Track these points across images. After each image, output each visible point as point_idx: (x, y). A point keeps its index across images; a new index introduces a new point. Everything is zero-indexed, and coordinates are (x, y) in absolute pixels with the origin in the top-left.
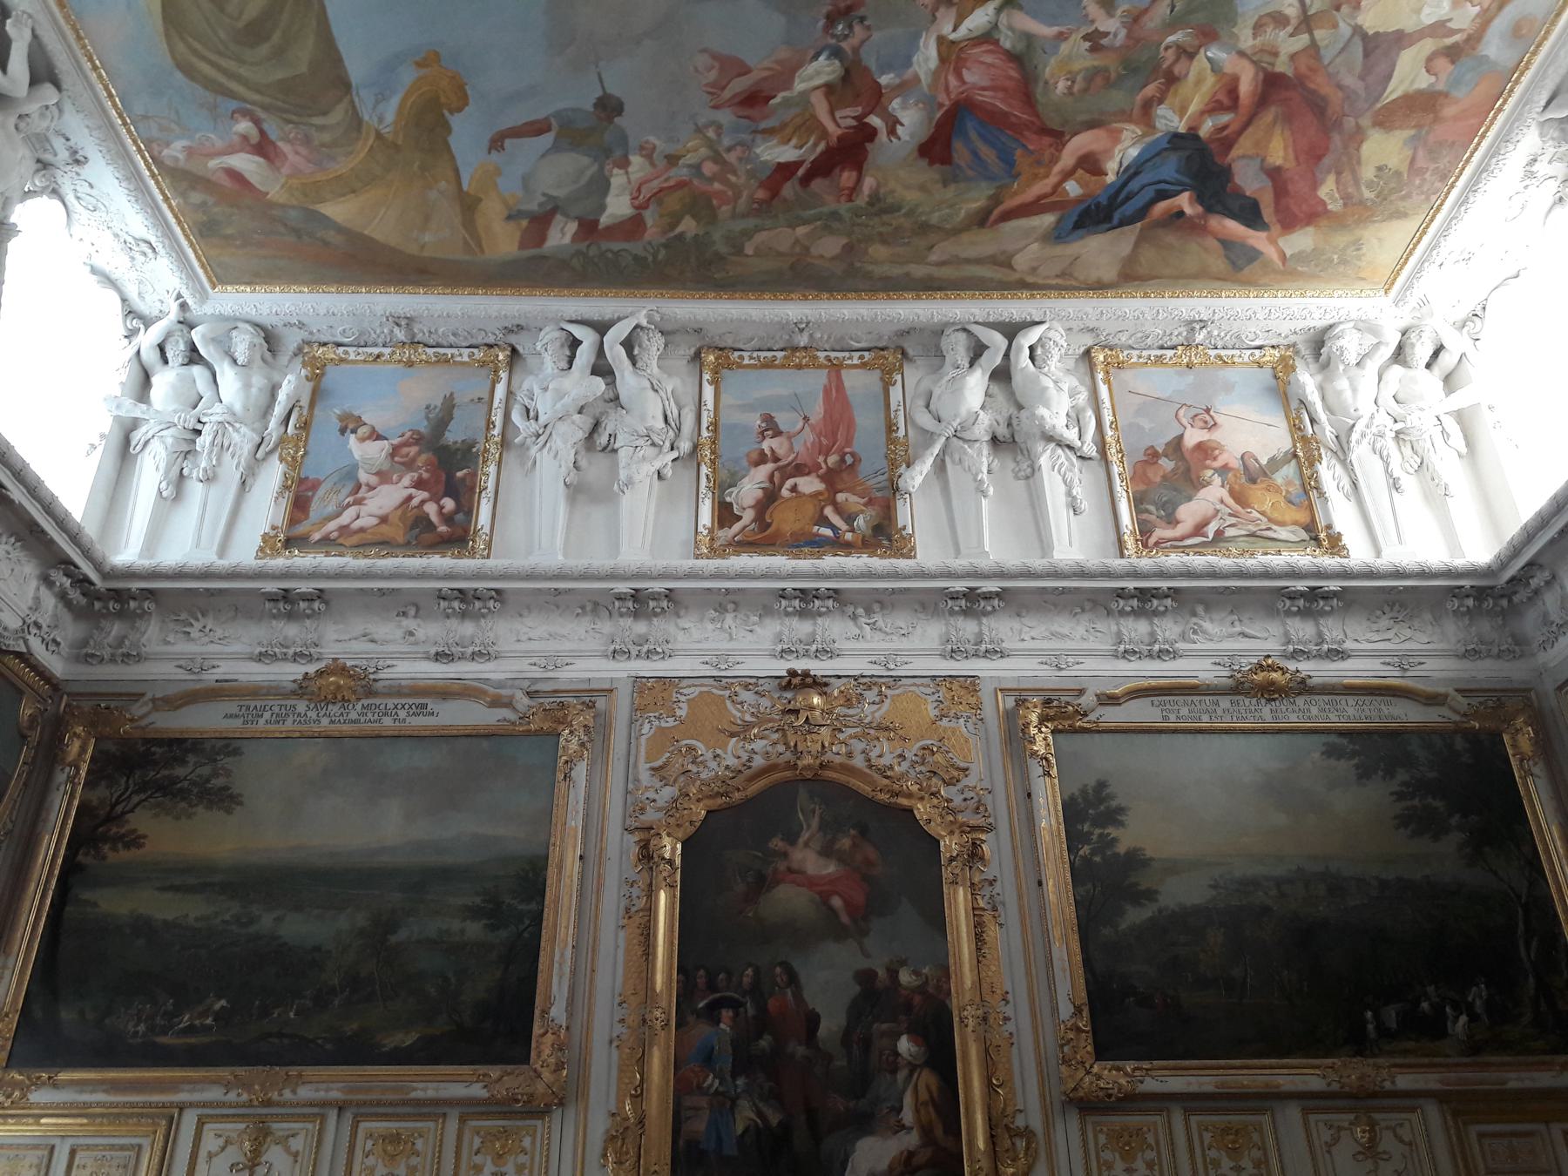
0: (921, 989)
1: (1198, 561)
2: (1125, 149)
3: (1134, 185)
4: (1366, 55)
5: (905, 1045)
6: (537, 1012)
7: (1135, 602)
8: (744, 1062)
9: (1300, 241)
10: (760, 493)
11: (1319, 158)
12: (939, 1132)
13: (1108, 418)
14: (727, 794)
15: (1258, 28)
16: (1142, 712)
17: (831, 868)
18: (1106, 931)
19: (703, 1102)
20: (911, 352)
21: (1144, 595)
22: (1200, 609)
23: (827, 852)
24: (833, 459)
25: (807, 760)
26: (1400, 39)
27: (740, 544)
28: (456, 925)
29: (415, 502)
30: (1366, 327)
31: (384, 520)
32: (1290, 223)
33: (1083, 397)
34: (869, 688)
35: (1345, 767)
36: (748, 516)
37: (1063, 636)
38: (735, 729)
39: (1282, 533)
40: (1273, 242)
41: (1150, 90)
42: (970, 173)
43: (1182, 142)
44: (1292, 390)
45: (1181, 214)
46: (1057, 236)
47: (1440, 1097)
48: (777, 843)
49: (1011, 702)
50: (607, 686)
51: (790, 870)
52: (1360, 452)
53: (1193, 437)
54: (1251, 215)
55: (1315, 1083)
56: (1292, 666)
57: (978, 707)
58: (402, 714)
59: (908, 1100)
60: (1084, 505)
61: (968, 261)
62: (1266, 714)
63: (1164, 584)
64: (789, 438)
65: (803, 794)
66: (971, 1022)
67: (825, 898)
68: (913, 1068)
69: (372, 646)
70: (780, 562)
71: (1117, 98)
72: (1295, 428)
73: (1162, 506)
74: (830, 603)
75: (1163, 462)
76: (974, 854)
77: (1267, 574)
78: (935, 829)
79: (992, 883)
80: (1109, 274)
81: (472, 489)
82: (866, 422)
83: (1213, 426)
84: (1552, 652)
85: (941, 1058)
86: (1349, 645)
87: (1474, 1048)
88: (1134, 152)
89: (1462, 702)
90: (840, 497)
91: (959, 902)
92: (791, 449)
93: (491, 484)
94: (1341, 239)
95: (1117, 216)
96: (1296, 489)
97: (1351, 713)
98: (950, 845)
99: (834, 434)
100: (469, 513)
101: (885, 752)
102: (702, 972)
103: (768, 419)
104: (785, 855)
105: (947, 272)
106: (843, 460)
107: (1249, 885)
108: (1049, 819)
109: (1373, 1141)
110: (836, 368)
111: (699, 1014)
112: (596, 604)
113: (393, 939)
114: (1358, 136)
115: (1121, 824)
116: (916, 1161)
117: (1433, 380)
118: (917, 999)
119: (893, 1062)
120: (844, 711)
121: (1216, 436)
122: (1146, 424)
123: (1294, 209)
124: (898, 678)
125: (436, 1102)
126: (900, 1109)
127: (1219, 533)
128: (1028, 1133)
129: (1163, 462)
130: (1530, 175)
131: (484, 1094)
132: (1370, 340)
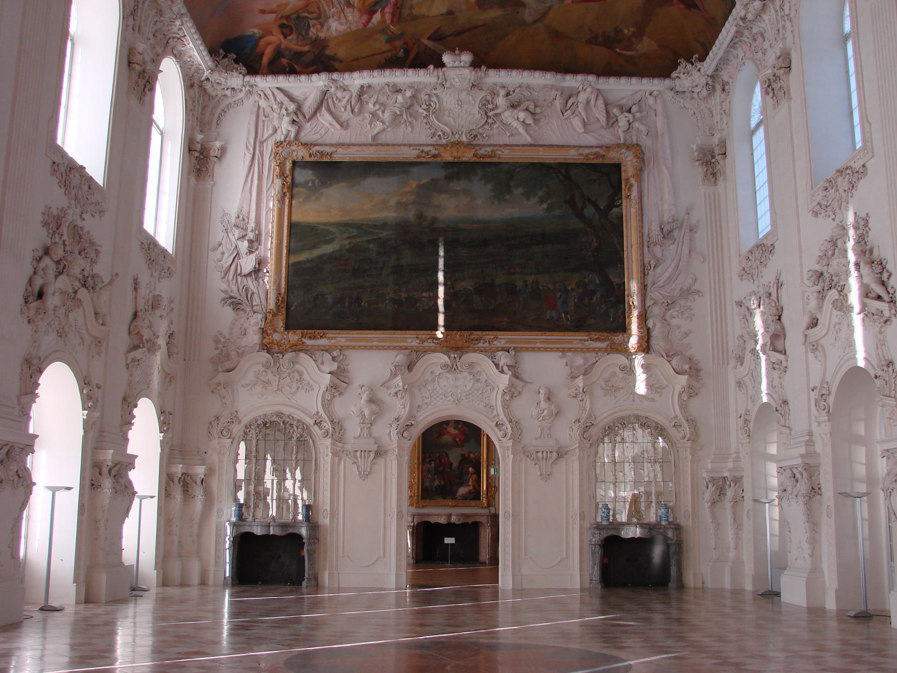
5: (471, 469)
17: (456, 432)
23: (455, 428)
67: (455, 438)
85: (478, 472)
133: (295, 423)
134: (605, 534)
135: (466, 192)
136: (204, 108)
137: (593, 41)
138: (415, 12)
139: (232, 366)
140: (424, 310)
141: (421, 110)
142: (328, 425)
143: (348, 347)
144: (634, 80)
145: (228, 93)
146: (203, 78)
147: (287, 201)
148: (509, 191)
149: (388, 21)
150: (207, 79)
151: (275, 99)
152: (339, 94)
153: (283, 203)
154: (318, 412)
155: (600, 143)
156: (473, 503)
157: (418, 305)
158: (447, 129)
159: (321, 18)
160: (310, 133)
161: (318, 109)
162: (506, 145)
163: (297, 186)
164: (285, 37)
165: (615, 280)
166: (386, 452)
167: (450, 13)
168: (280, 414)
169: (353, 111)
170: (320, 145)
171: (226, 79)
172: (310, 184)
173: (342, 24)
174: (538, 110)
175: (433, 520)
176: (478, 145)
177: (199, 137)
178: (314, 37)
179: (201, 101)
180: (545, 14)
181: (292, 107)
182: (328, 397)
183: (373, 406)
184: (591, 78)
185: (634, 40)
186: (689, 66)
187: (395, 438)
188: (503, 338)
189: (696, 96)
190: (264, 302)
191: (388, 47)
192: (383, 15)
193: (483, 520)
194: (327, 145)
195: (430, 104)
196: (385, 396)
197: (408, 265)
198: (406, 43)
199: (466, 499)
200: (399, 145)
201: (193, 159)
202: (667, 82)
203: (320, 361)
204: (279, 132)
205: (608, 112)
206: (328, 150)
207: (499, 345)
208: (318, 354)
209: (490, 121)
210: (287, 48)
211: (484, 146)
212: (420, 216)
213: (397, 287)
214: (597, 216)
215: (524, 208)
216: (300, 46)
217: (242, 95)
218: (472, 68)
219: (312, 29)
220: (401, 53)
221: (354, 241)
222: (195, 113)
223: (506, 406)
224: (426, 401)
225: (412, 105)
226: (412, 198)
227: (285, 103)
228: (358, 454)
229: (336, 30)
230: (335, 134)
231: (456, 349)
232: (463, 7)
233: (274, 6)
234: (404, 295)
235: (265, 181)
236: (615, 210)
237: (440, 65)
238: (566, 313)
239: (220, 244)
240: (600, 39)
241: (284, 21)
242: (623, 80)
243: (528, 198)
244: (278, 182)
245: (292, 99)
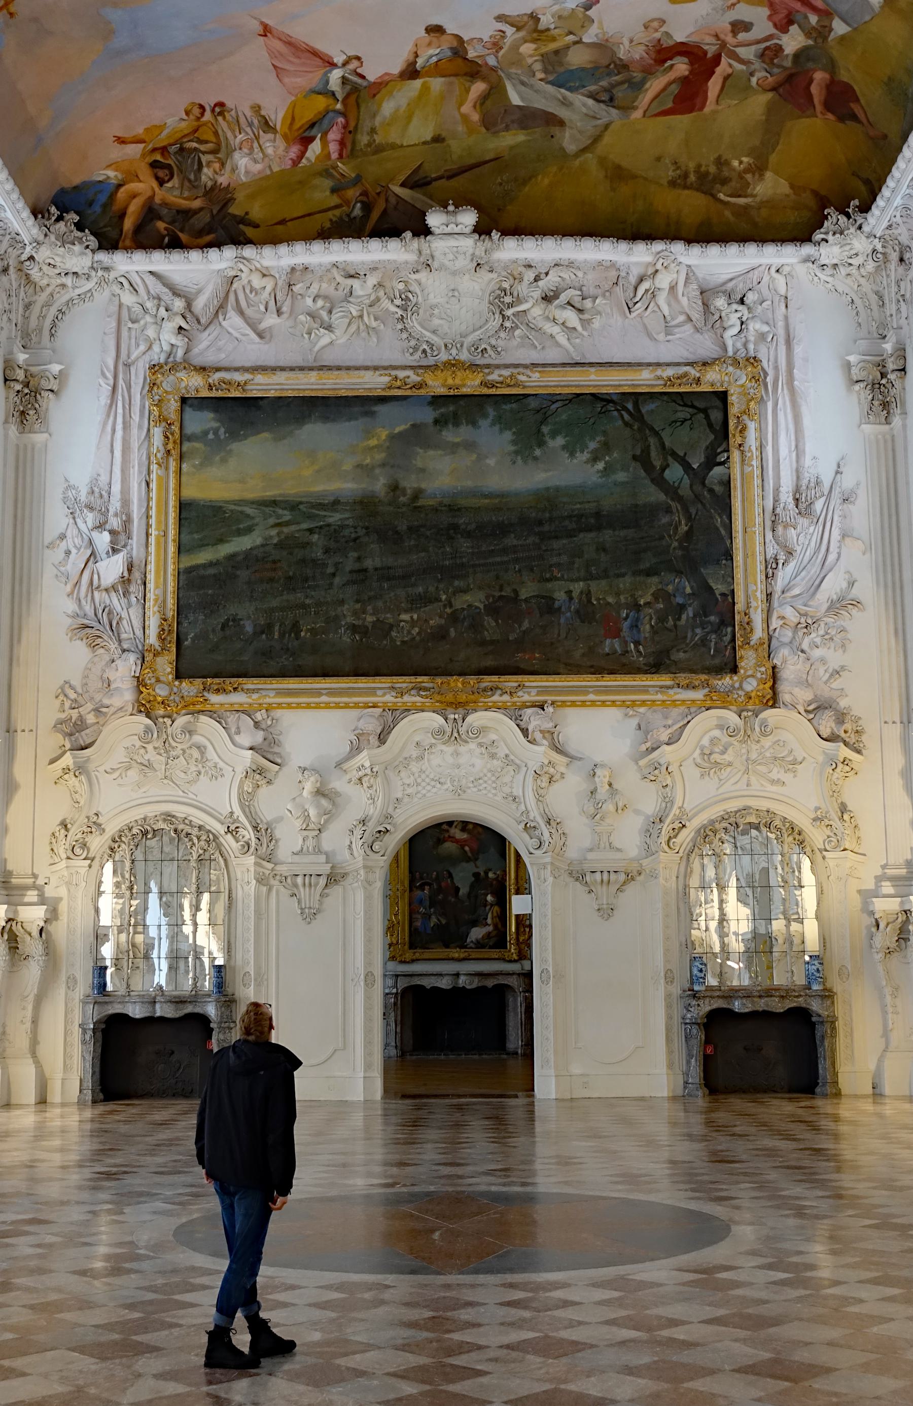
0: (496, 879)
5: (489, 898)
17: (465, 836)
59: (490, 916)
67: (462, 847)
68: (492, 905)
104: (448, 831)
111: (417, 888)
133: (195, 832)
134: (706, 1007)
135: (470, 446)
136: (27, 307)
137: (679, 182)
138: (378, 139)
139: (88, 741)
140: (403, 642)
141: (393, 309)
142: (248, 834)
143: (280, 706)
144: (751, 249)
145: (68, 281)
146: (24, 257)
147: (173, 465)
148: (541, 444)
149: (334, 156)
150: (31, 258)
151: (148, 292)
152: (257, 282)
153: (167, 469)
154: (232, 813)
155: (692, 358)
156: (495, 953)
157: (394, 634)
158: (435, 339)
159: (220, 150)
160: (208, 347)
161: (221, 308)
162: (534, 365)
163: (189, 439)
164: (161, 183)
165: (719, 588)
166: (344, 876)
167: (438, 139)
168: (169, 817)
169: (279, 312)
170: (227, 369)
171: (63, 257)
172: (211, 436)
173: (256, 161)
174: (588, 304)
175: (428, 983)
176: (488, 366)
177: (22, 357)
178: (210, 184)
179: (22, 294)
180: (597, 139)
181: (179, 304)
182: (248, 787)
183: (324, 802)
184: (678, 248)
185: (749, 177)
186: (843, 219)
187: (358, 851)
188: (534, 687)
189: (854, 271)
190: (139, 633)
191: (335, 200)
192: (325, 143)
193: (513, 982)
194: (237, 369)
195: (407, 298)
196: (339, 784)
197: (376, 569)
198: (365, 193)
199: (483, 947)
200: (357, 368)
201: (12, 394)
202: (807, 250)
203: (233, 730)
204: (156, 348)
205: (705, 305)
206: (238, 377)
207: (526, 698)
208: (232, 719)
209: (508, 324)
210: (165, 204)
211: (498, 367)
212: (395, 488)
213: (358, 606)
214: (686, 481)
215: (569, 470)
216: (184, 199)
217: (90, 285)
218: (476, 236)
219: (205, 170)
220: (357, 211)
221: (286, 530)
222: (13, 316)
223: (539, 798)
224: (409, 791)
225: (378, 299)
226: (380, 456)
227: (165, 298)
228: (299, 880)
229: (247, 172)
230: (253, 351)
231: (457, 705)
232: (460, 128)
233: (140, 131)
234: (370, 619)
235: (135, 431)
236: (717, 470)
237: (423, 231)
238: (637, 643)
239: (62, 537)
240: (692, 178)
241: (158, 157)
242: (733, 249)
243: (572, 454)
244: (157, 433)
245: (176, 292)
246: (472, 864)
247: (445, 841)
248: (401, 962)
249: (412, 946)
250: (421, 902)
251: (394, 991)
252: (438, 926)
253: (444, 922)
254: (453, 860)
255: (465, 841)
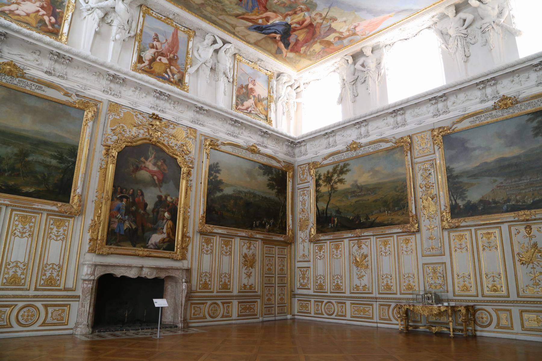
0: (172, 202)
1: (245, 116)
2: (276, 20)
3: (272, 28)
4: (328, 30)
5: (166, 214)
6: (73, 190)
7: (233, 122)
8: (128, 212)
9: (291, 55)
10: (151, 57)
11: (307, 42)
12: (171, 235)
13: (236, 73)
14: (131, 143)
15: (317, 14)
16: (228, 149)
17: (155, 169)
18: (212, 196)
19: (116, 220)
20: (197, 34)
21: (236, 121)
22: (244, 128)
23: (155, 164)
24: (172, 55)
25: (154, 139)
26: (335, 31)
27: (143, 70)
28: (48, 159)
29: (41, 13)
30: (289, 76)
31: (28, 15)
32: (292, 51)
33: (232, 65)
34: (172, 124)
35: (262, 171)
36: (147, 63)
37: (216, 125)
38: (135, 125)
39: (262, 116)
40: (287, 52)
41: (290, 13)
42: (243, 5)
43: (288, 25)
44: (270, 83)
45: (276, 38)
46: (249, 28)
47: (262, 239)
48: (143, 159)
49: (203, 138)
50: (100, 100)
51: (145, 167)
52: (279, 103)
53: (251, 86)
54: (287, 45)
55: (244, 234)
56: (258, 147)
57: (196, 137)
58: (33, 88)
59: (165, 227)
60: (227, 94)
61: (227, 22)
62: (251, 156)
63: (241, 121)
64: (161, 44)
65: (151, 148)
66: (182, 212)
67: (153, 176)
68: (167, 220)
69: (21, 60)
70: (153, 80)
71: (283, 10)
72: (269, 92)
73: (241, 100)
74: (166, 98)
75: (244, 89)
76: (189, 173)
77: (260, 126)
78: (181, 165)
79: (191, 181)
80: (252, 41)
81: (62, 18)
82: (182, 47)
83: (255, 85)
84: (299, 158)
85: (174, 219)
86: (268, 146)
87: (269, 231)
88: (277, 22)
89: (283, 164)
90: (172, 67)
91: (183, 184)
92: (161, 47)
93: (69, 19)
94: (298, 58)
95: (264, 31)
96: (266, 107)
97: (265, 160)
98: (184, 169)
99: (173, 48)
100: (60, 25)
101: (173, 142)
102: (119, 188)
103: (156, 35)
104: (144, 163)
105: (220, 22)
106: (174, 57)
107: (240, 192)
108: (205, 169)
109: (250, 246)
110: (177, 29)
111: (117, 199)
112: (100, 73)
113: (27, 159)
114: (315, 42)
115: (219, 173)
116: (165, 241)
117: (294, 93)
118: (171, 204)
119: (163, 218)
120: (164, 128)
121: (255, 88)
122: (242, 78)
123: (295, 49)
124: (178, 124)
125: (40, 209)
126: (163, 229)
127: (250, 111)
128: (189, 237)
129: (244, 89)
130: (333, 64)
131: (57, 209)
132: (289, 79)
156: (167, 254)
175: (119, 273)
199: (159, 249)
246: (158, 188)
247: (141, 169)
248: (99, 254)
249: (108, 242)
250: (119, 210)
251: (92, 278)
252: (129, 230)
253: (134, 227)
254: (146, 184)
255: (155, 172)
